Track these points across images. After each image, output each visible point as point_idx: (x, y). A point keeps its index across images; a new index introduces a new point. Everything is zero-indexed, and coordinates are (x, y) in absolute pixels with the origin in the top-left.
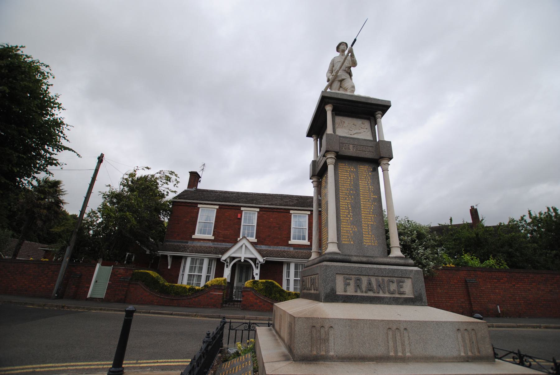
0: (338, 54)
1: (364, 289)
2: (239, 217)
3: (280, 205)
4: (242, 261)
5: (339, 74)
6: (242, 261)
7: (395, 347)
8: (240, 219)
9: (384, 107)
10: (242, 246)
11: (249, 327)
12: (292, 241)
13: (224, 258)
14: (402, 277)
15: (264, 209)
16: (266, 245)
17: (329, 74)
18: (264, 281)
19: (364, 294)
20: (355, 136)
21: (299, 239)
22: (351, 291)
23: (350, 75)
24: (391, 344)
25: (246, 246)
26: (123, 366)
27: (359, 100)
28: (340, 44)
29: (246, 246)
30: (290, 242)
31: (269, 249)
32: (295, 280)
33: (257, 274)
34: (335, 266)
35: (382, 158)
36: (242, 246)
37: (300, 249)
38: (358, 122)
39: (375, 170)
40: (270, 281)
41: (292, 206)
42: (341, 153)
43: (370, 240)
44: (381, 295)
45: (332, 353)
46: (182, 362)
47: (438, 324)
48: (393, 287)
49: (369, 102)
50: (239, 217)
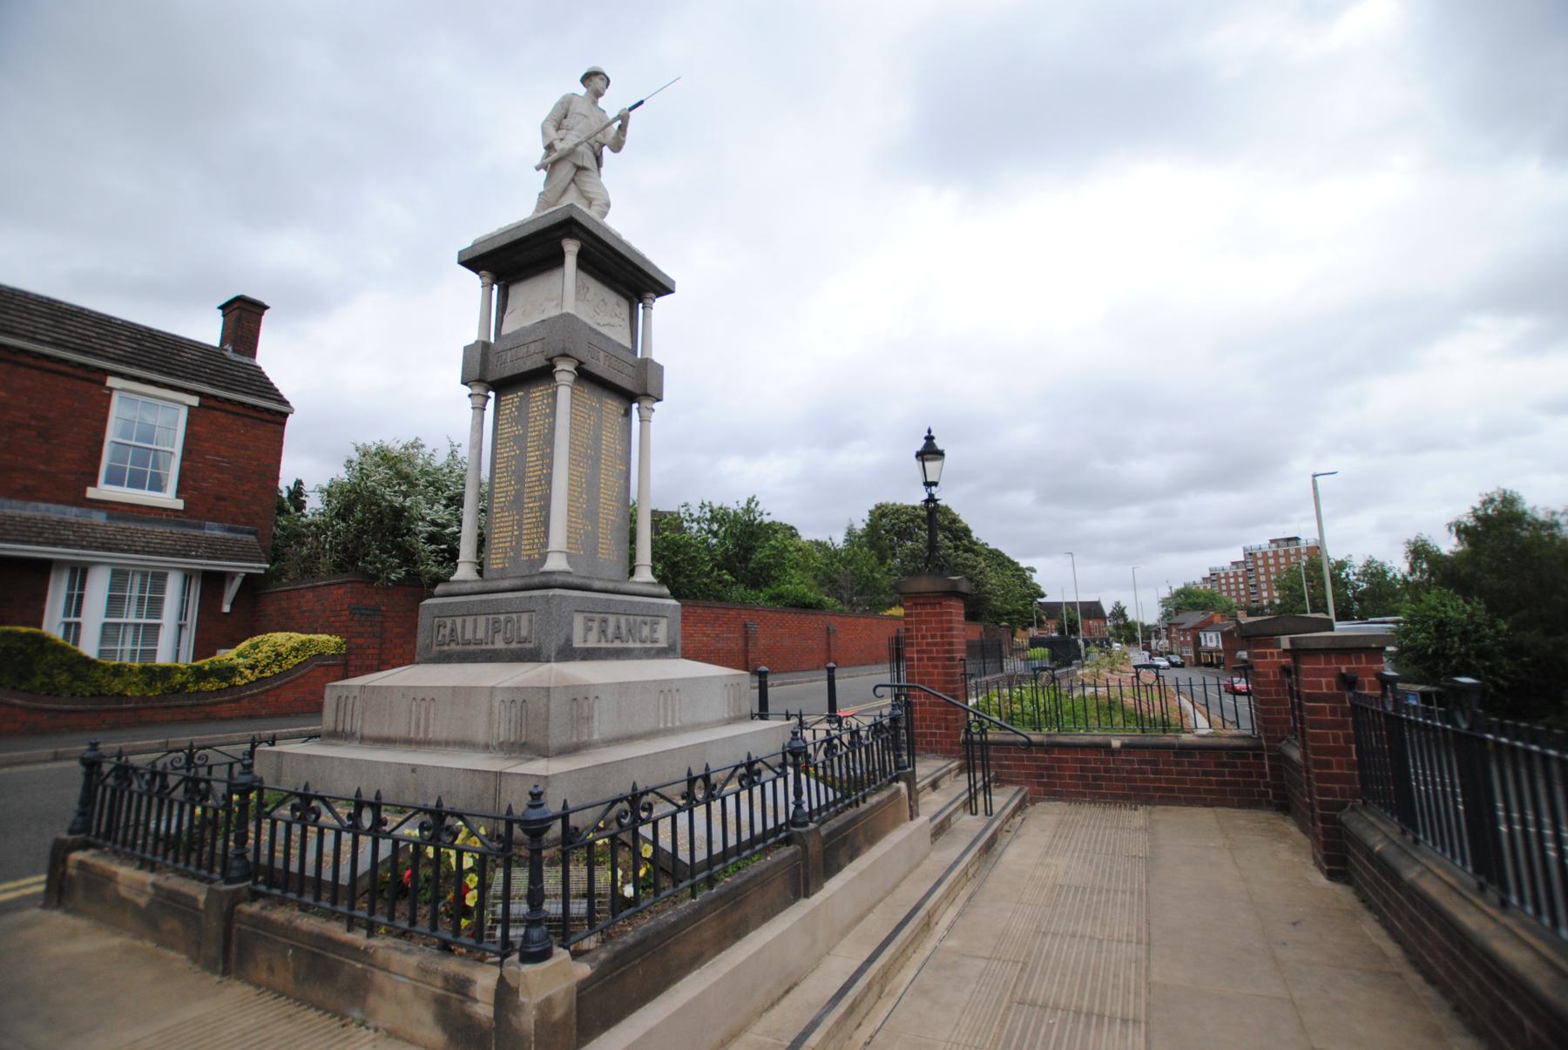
0: (582, 91)
1: (610, 636)
3: (55, 344)
5: (580, 148)
7: (666, 716)
9: (662, 288)
12: (103, 491)
14: (658, 615)
19: (609, 645)
20: (604, 330)
21: (137, 482)
23: (598, 159)
24: (662, 712)
27: (637, 262)
30: (91, 493)
32: (105, 625)
34: (575, 598)
35: (647, 395)
37: (143, 521)
38: (612, 298)
39: (628, 413)
40: (24, 629)
43: (609, 552)
44: (631, 645)
45: (596, 737)
47: (709, 679)
48: (646, 631)
49: (646, 269)
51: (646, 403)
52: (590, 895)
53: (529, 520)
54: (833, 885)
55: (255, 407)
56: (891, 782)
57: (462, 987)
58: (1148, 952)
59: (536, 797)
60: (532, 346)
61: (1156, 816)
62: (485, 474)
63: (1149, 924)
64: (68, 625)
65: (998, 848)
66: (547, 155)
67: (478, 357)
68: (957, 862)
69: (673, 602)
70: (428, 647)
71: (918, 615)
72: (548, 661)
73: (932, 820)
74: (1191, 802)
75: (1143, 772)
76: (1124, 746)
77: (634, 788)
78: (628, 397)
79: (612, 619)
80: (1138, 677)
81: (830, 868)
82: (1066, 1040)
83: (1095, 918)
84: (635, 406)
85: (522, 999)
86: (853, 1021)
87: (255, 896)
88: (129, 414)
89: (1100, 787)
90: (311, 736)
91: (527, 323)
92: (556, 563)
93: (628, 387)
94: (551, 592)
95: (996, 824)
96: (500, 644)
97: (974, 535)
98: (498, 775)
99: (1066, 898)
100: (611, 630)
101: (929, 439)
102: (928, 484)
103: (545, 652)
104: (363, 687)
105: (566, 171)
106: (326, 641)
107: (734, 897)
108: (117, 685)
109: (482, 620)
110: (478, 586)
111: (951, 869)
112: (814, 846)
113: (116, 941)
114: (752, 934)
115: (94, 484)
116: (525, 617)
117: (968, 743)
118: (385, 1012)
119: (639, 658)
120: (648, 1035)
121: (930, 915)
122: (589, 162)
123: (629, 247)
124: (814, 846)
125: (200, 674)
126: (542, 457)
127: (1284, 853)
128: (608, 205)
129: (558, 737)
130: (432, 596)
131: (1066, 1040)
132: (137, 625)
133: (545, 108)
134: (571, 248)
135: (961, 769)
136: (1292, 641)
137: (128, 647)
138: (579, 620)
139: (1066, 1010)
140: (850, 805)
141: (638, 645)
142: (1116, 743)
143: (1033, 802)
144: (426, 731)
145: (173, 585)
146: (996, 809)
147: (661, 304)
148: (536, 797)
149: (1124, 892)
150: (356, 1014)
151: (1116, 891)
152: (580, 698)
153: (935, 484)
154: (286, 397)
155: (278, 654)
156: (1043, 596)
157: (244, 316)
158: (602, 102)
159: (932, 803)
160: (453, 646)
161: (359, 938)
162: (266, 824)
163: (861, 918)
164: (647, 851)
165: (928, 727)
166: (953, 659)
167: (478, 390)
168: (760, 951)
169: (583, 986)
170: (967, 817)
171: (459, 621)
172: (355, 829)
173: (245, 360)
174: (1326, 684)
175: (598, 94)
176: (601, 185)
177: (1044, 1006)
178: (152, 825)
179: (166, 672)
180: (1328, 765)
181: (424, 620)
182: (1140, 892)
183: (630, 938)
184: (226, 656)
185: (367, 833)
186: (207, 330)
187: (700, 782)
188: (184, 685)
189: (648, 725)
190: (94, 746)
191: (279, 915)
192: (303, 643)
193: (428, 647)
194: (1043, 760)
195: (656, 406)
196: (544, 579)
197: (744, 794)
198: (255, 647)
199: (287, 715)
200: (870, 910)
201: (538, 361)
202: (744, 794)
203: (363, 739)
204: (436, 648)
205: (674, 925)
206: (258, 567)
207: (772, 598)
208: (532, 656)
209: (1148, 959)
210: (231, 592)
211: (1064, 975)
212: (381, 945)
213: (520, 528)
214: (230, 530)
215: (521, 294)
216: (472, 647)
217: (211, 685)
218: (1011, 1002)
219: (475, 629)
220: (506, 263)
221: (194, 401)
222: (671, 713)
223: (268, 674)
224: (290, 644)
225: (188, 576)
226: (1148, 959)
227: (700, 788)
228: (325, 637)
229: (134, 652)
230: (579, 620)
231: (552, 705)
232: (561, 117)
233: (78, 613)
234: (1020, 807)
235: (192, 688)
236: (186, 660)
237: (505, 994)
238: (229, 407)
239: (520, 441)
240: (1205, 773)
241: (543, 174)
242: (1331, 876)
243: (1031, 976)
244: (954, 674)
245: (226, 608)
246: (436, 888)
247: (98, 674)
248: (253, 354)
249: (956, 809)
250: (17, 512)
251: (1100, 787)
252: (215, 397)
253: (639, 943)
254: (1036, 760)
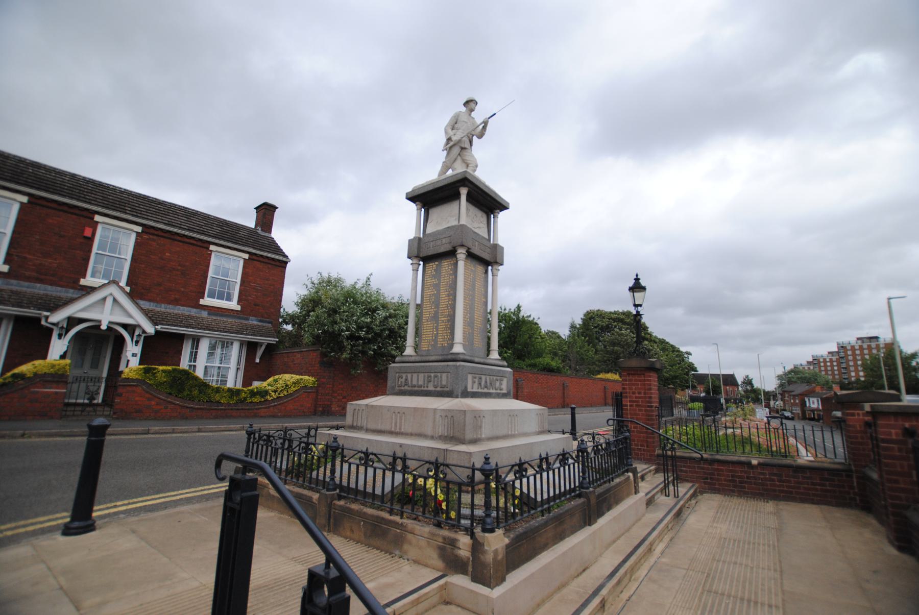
0: (464, 109)
2: (88, 232)
3: (189, 230)
4: (104, 327)
6: (104, 327)
8: (91, 239)
9: (503, 207)
10: (105, 299)
11: (285, 433)
12: (206, 301)
13: (59, 317)
14: (502, 375)
15: (152, 231)
16: (150, 300)
17: (450, 131)
18: (170, 368)
20: (476, 230)
21: (221, 297)
22: (475, 390)
25: (115, 300)
26: (94, 514)
27: (493, 196)
28: (472, 101)
29: (115, 300)
30: (202, 302)
31: (158, 309)
33: (134, 355)
36: (105, 299)
37: (222, 316)
39: (486, 272)
41: (215, 238)
43: (479, 343)
44: (491, 391)
46: (142, 501)
47: (530, 410)
50: (88, 232)
51: (495, 267)
52: (498, 508)
53: (442, 326)
54: (602, 521)
55: (273, 259)
56: (623, 473)
57: (453, 543)
58: (781, 575)
59: (487, 459)
60: (444, 241)
61: (781, 507)
62: (419, 302)
63: (780, 562)
64: (190, 366)
65: (684, 515)
66: (447, 144)
67: (416, 245)
68: (662, 520)
69: (509, 369)
70: (393, 388)
71: (630, 380)
72: (457, 397)
73: (647, 494)
74: (803, 500)
75: (773, 480)
76: (759, 464)
77: (520, 460)
78: (486, 263)
79: (483, 377)
80: (769, 423)
81: (600, 514)
82: (737, 611)
83: (747, 556)
84: (490, 268)
85: (486, 548)
86: (619, 589)
87: (340, 497)
88: (218, 263)
89: (744, 487)
90: (332, 428)
91: (440, 228)
92: (458, 349)
93: (488, 259)
94: (458, 363)
95: (682, 503)
96: (431, 388)
97: (650, 330)
98: (446, 451)
99: (729, 545)
100: (483, 383)
101: (637, 280)
102: (636, 306)
103: (455, 393)
104: (367, 405)
105: (456, 150)
106: (308, 379)
107: (559, 519)
108: (217, 397)
109: (421, 375)
110: (418, 359)
111: (659, 523)
112: (593, 500)
113: (272, 514)
114: (567, 539)
115: (203, 298)
116: (444, 375)
117: (665, 457)
118: (413, 552)
119: (494, 398)
120: (532, 575)
121: (651, 544)
122: (467, 145)
123: (489, 189)
124: (593, 500)
125: (253, 394)
126: (449, 295)
127: (867, 534)
128: (477, 166)
129: (469, 435)
130: (394, 362)
131: (737, 611)
132: (219, 368)
133: (446, 120)
134: (464, 192)
135: (657, 471)
136: (871, 406)
137: (215, 378)
138: (470, 377)
139: (735, 597)
140: (605, 482)
141: (494, 391)
142: (754, 462)
143: (702, 493)
144: (400, 428)
145: (236, 347)
146: (681, 495)
147: (502, 216)
148: (487, 459)
149: (764, 545)
150: (397, 552)
151: (759, 544)
152: (477, 415)
153: (641, 305)
154: (287, 254)
155: (287, 385)
156: (695, 370)
157: (266, 212)
158: (473, 114)
159: (644, 487)
160: (406, 388)
161: (397, 518)
162: (346, 466)
163: (614, 542)
164: (518, 493)
165: (637, 445)
166: (652, 407)
167: (415, 261)
168: (573, 547)
169: (507, 546)
170: (663, 498)
171: (409, 375)
172: (393, 470)
173: (267, 235)
174: (894, 434)
175: (472, 110)
176: (473, 156)
177: (723, 594)
178: (278, 465)
179: (238, 392)
180: (896, 482)
181: (391, 374)
182: (774, 546)
183: (520, 530)
184: (256, 384)
185: (400, 471)
186: (249, 221)
188: (245, 398)
189: (504, 432)
190: (251, 425)
191: (355, 507)
192: (298, 380)
193: (393, 388)
194: (708, 469)
195: (500, 268)
196: (453, 357)
197: (562, 469)
198: (276, 381)
199: (289, 416)
200: (618, 538)
201: (446, 248)
202: (562, 469)
203: (367, 430)
204: (397, 388)
205: (537, 527)
206: (273, 340)
207: (530, 365)
208: (449, 394)
209: (782, 579)
210: (260, 352)
211: (732, 581)
212: (405, 521)
213: (437, 330)
214: (260, 321)
215: (435, 213)
216: (416, 389)
217: (257, 399)
218: (703, 590)
219: (418, 380)
220: (428, 199)
221: (246, 256)
222: (516, 428)
223: (282, 395)
224: (292, 380)
225: (242, 343)
226: (782, 579)
227: (544, 463)
228: (306, 377)
229: (217, 381)
230: (470, 377)
231: (467, 419)
232: (454, 124)
233: (195, 361)
234: (694, 495)
235: (249, 400)
236: (239, 386)
237: (477, 547)
238: (261, 259)
239: (437, 286)
240: (813, 484)
241: (445, 152)
242: (900, 549)
243: (713, 578)
244: (652, 415)
245: (258, 361)
246: (425, 500)
247: (210, 391)
248: (270, 232)
249: (657, 492)
250: (171, 311)
251: (744, 487)
252: (255, 254)
253: (525, 533)
254: (703, 468)
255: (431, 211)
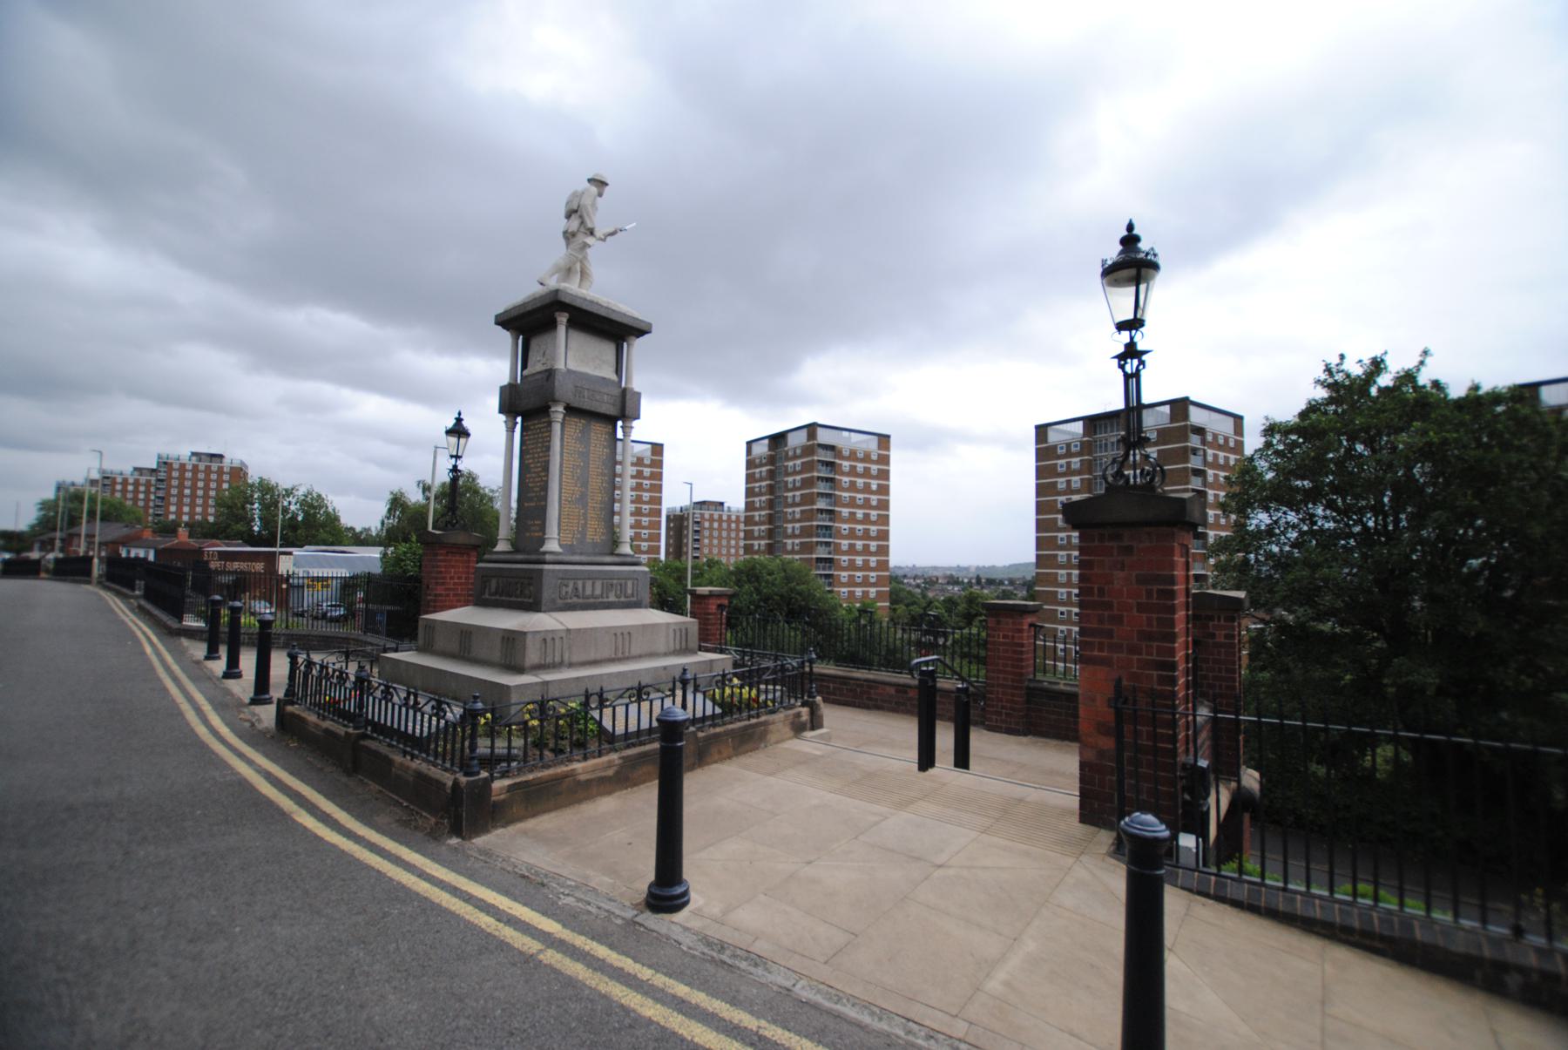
9: (640, 331)
42: (575, 405)
78: (611, 420)
84: (620, 423)
134: (562, 319)
172: (406, 705)
187: (595, 698)
220: (530, 323)
255: (534, 343)
